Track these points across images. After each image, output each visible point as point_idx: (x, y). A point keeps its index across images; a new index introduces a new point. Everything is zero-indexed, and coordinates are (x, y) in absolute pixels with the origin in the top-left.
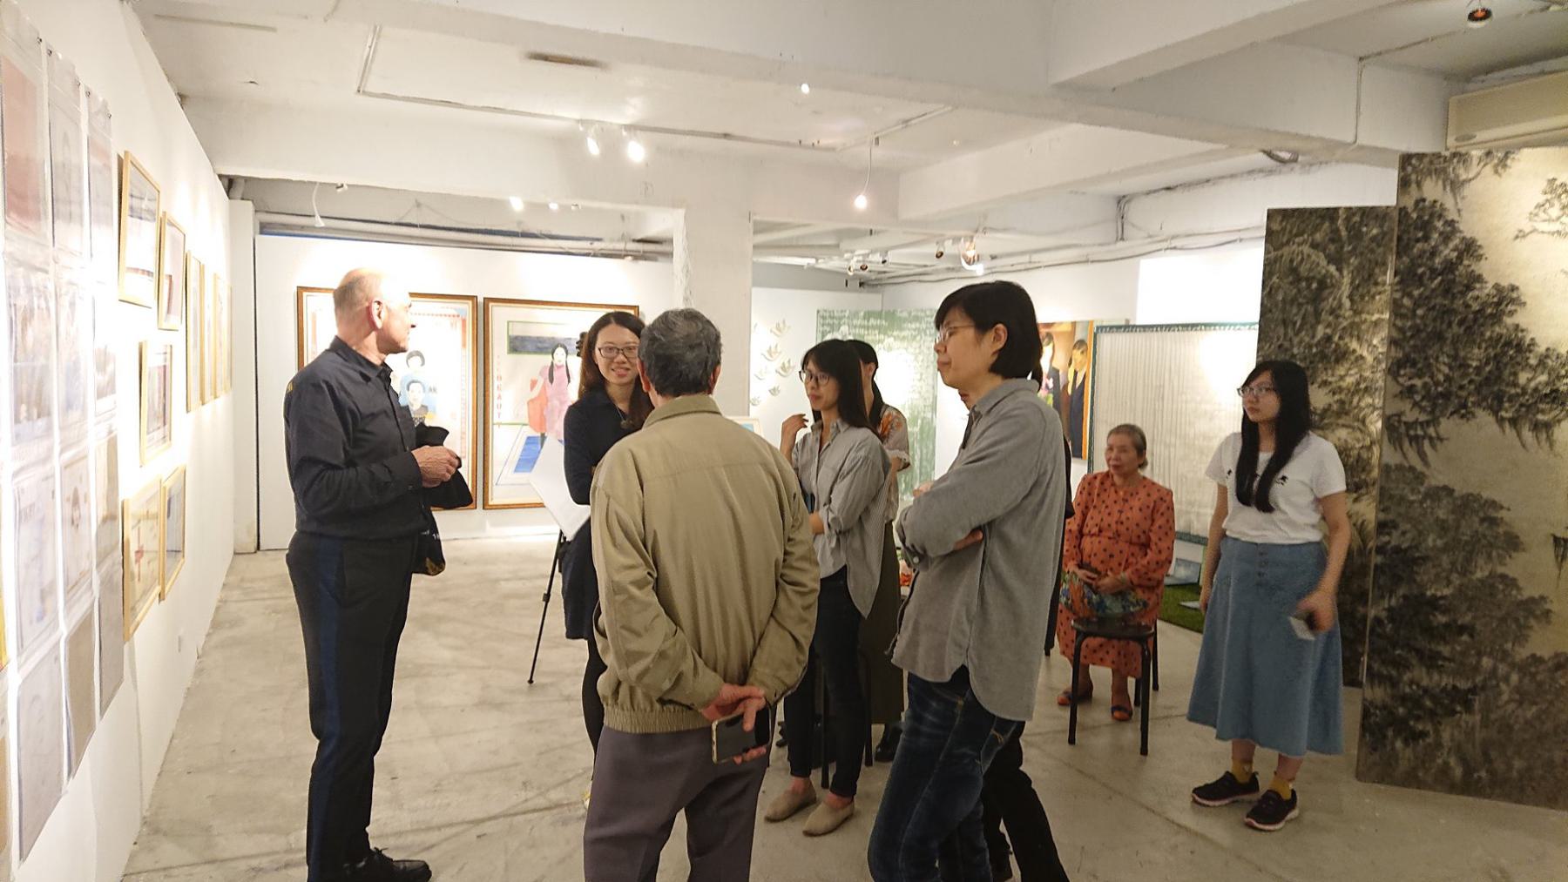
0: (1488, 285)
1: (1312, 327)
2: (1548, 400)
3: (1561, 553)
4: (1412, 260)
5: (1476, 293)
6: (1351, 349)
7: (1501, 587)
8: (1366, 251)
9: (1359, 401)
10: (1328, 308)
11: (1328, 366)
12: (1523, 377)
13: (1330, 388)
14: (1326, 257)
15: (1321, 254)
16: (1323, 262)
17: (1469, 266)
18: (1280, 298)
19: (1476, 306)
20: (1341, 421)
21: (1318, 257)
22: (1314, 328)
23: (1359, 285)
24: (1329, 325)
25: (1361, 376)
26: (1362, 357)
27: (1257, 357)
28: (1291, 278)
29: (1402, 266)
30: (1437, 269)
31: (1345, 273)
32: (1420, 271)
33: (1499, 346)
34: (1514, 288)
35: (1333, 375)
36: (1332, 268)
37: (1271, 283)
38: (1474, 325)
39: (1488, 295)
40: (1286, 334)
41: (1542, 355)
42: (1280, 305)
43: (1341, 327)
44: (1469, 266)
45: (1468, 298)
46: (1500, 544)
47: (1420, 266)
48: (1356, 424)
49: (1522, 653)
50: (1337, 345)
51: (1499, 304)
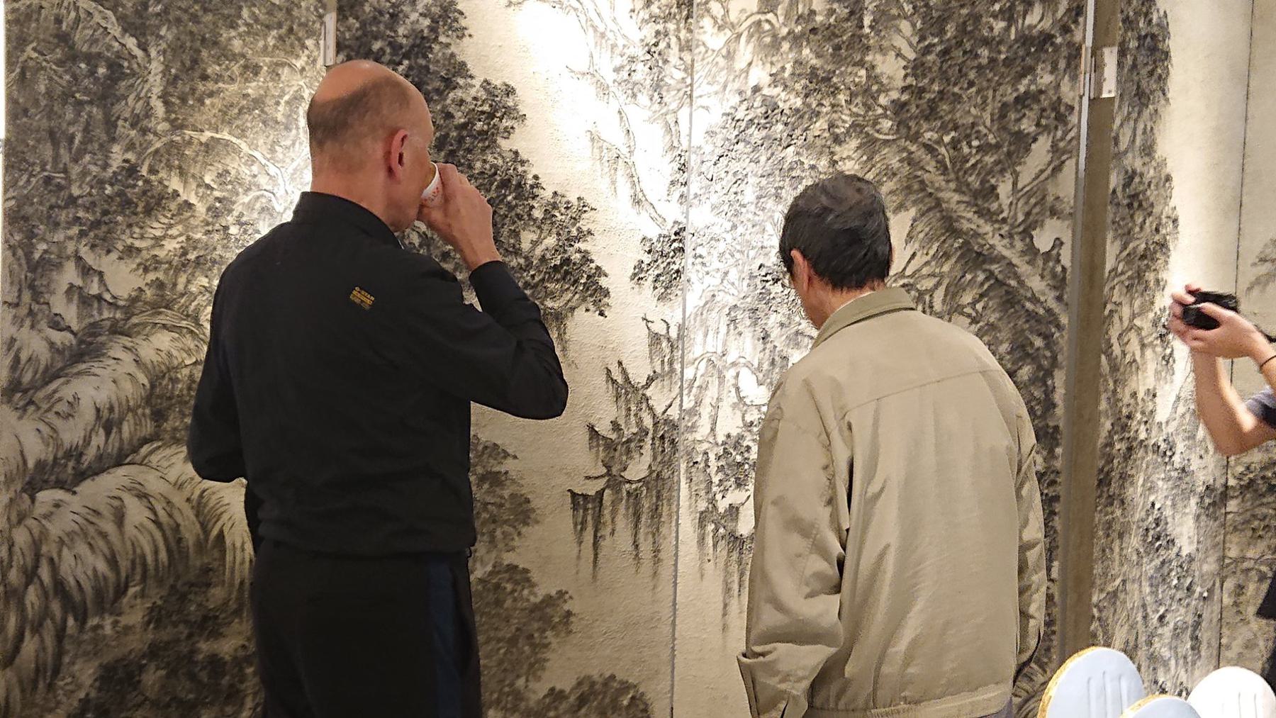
0: (473, 82)
1: (101, 146)
2: (558, 276)
3: (580, 520)
4: (363, 25)
5: (459, 93)
6: (170, 190)
7: (509, 587)
8: (185, 17)
9: (189, 281)
10: (127, 115)
11: (134, 219)
12: (527, 238)
13: (138, 260)
14: (117, 20)
15: (109, 13)
16: (116, 30)
17: (448, 45)
18: (42, 89)
19: (460, 119)
20: (160, 320)
21: (105, 18)
22: (105, 150)
23: (176, 77)
24: (131, 147)
25: (188, 238)
26: (188, 205)
27: (6, 200)
28: (59, 54)
29: (347, 35)
30: (401, 47)
31: (153, 53)
32: (377, 46)
33: (494, 187)
34: (510, 91)
35: (142, 237)
36: (131, 42)
37: (21, 59)
38: (458, 149)
39: (475, 99)
40: (56, 158)
41: (548, 204)
42: (43, 103)
43: (152, 149)
44: (448, 45)
45: (449, 101)
46: (505, 517)
47: (376, 38)
48: (184, 323)
49: (538, 691)
50: (147, 182)
51: (491, 116)
